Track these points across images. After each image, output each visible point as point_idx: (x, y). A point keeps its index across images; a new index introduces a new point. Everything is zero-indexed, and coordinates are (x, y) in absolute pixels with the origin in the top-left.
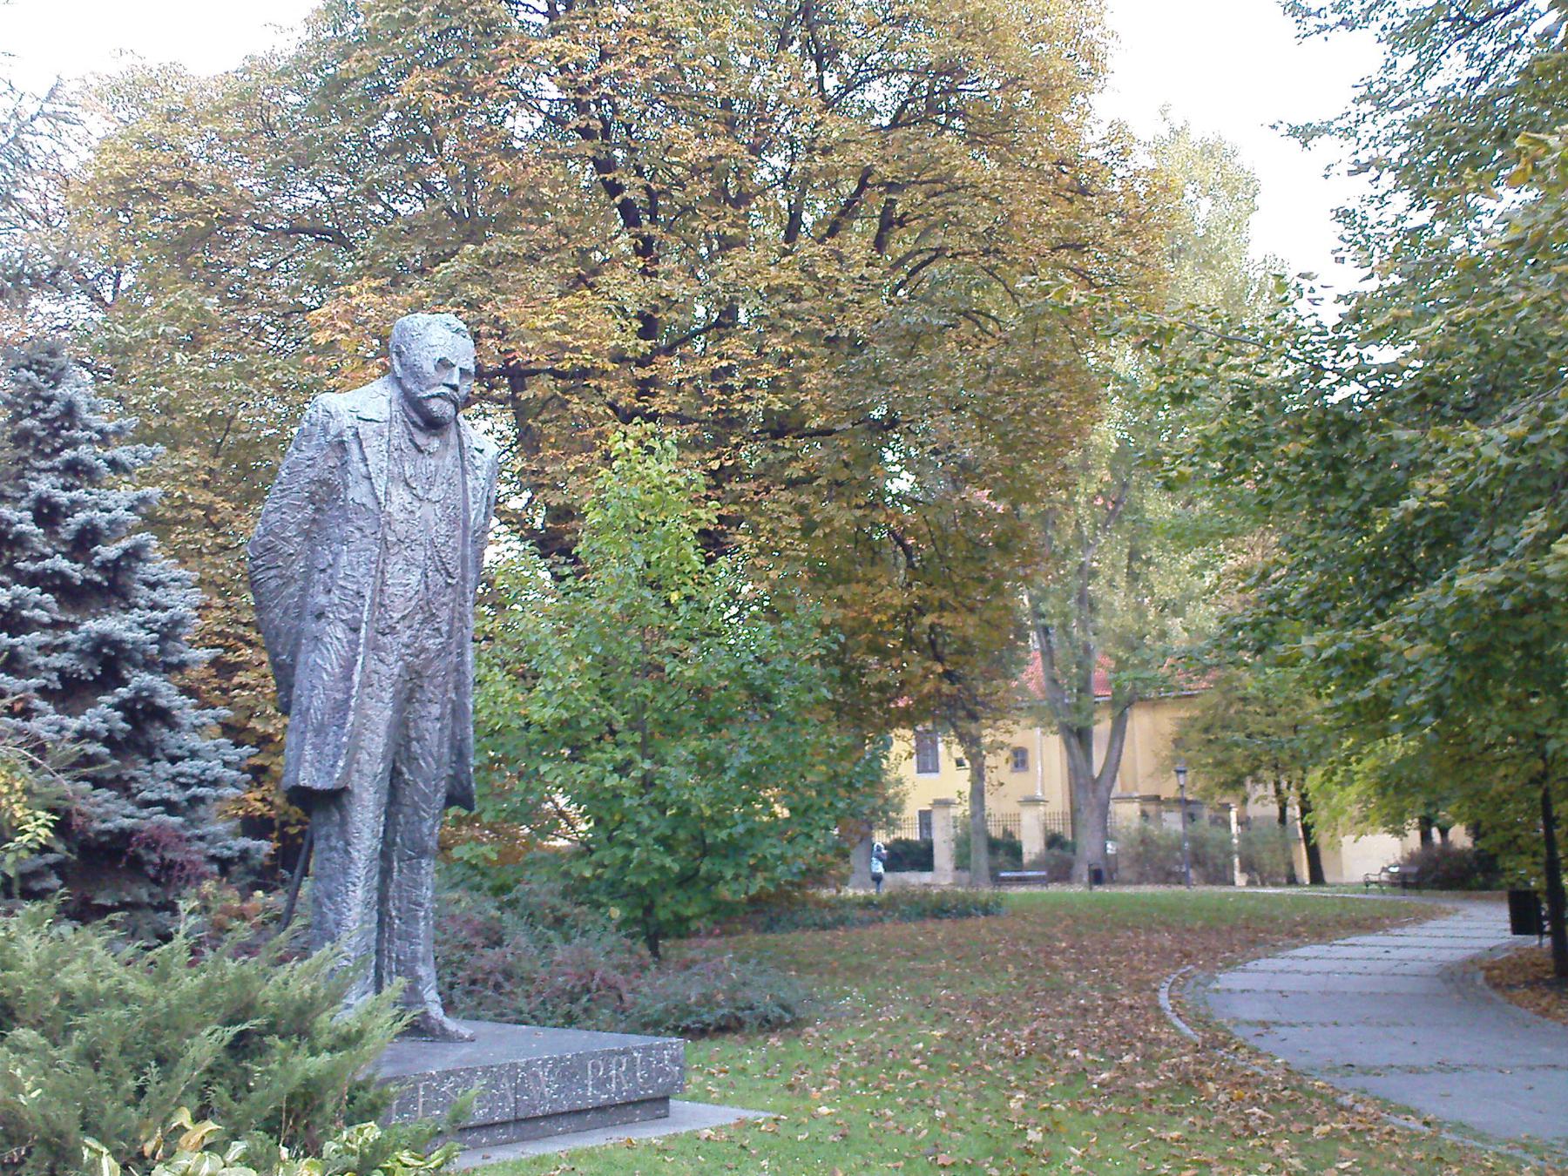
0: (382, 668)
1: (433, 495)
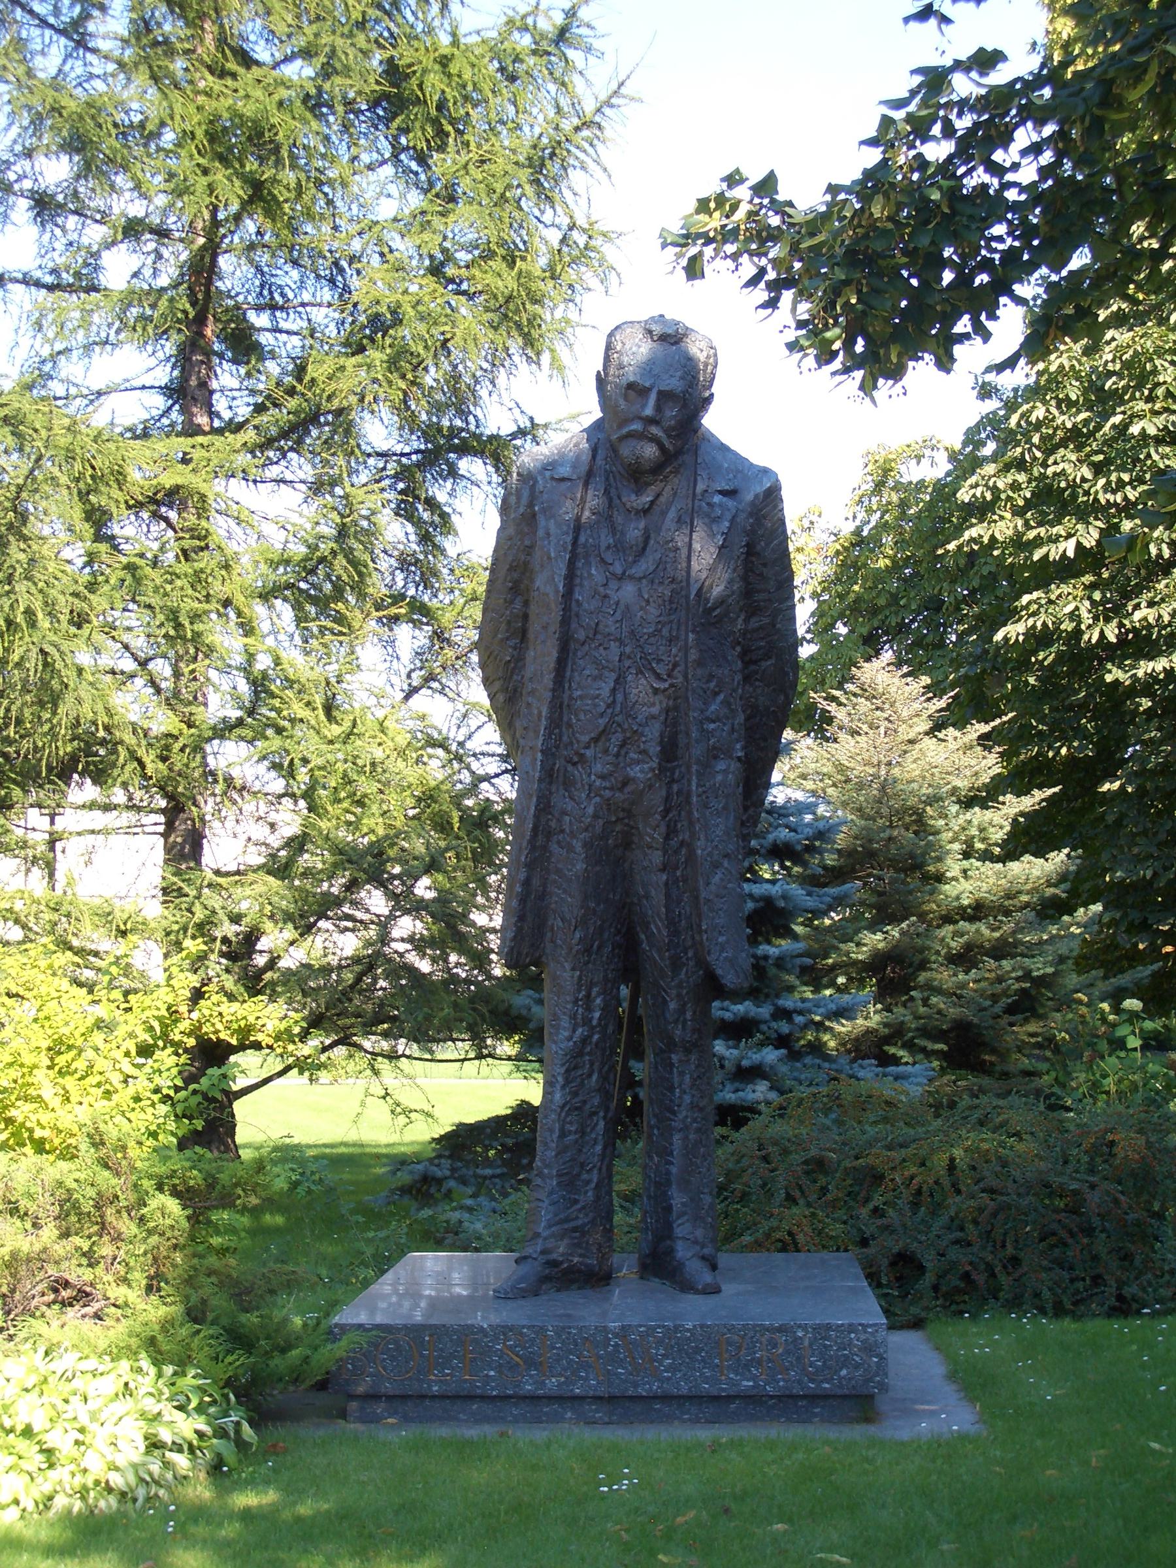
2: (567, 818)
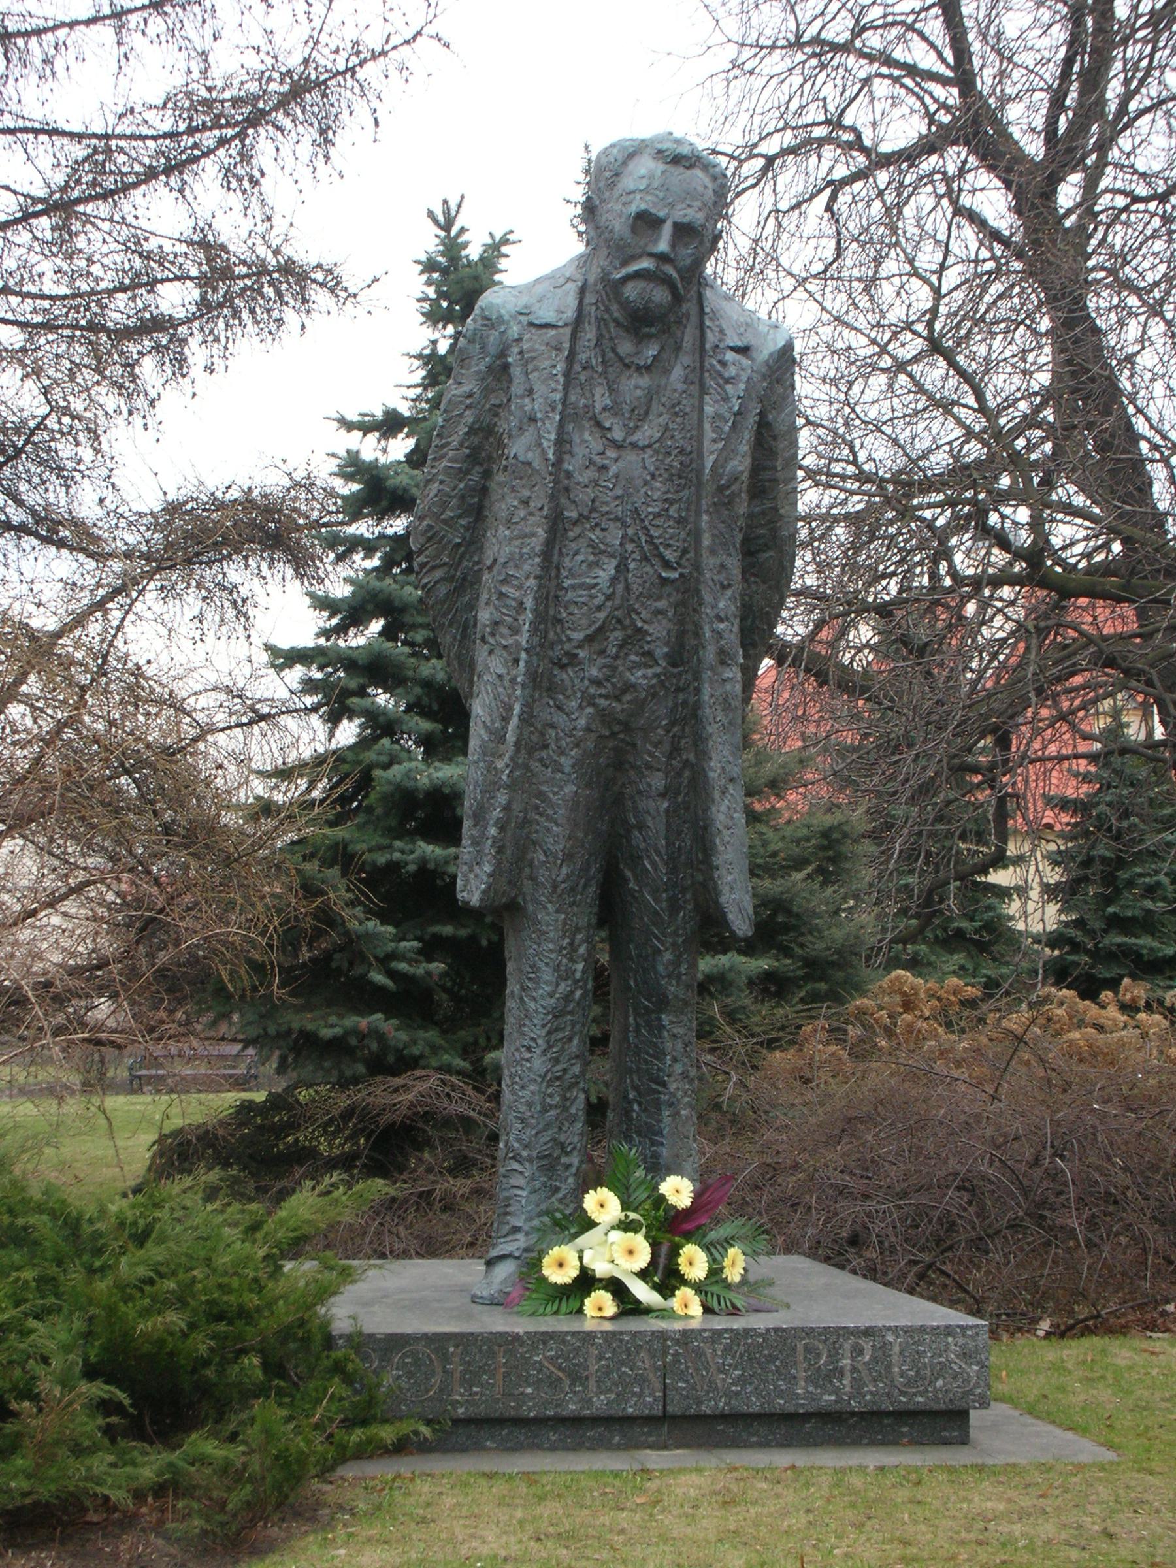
0: (560, 719)
2: (553, 733)
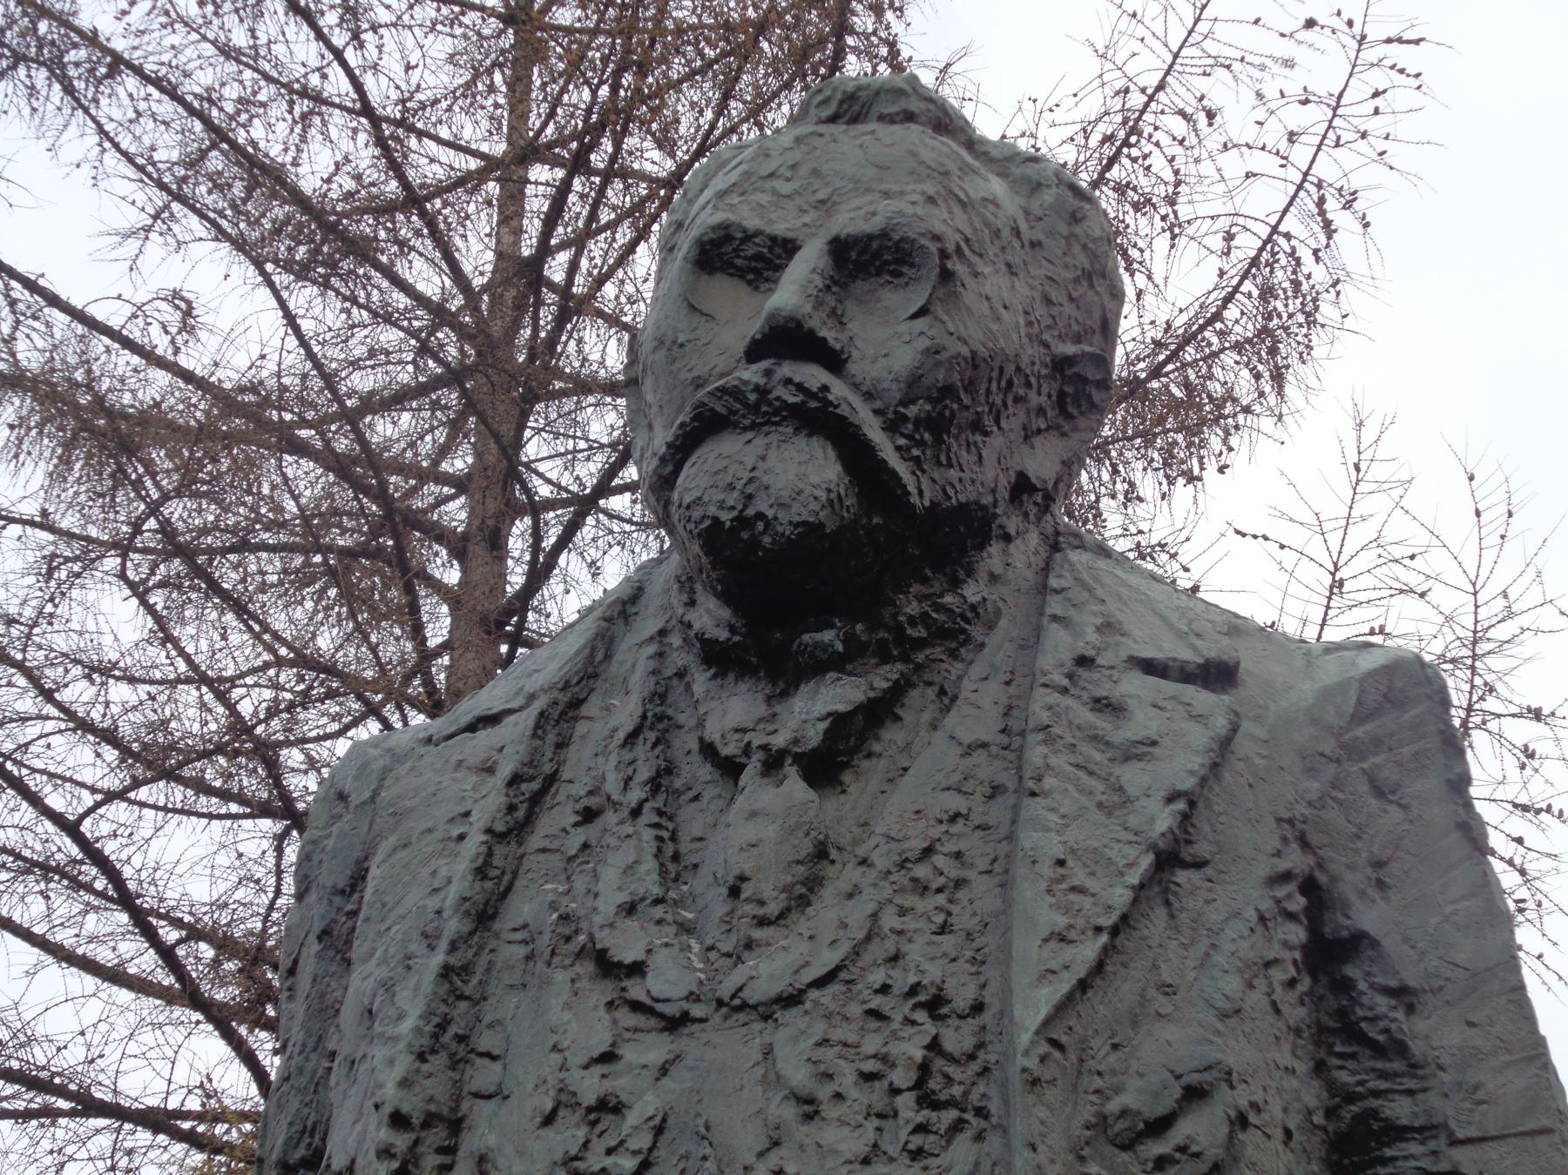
1: (767, 973)
